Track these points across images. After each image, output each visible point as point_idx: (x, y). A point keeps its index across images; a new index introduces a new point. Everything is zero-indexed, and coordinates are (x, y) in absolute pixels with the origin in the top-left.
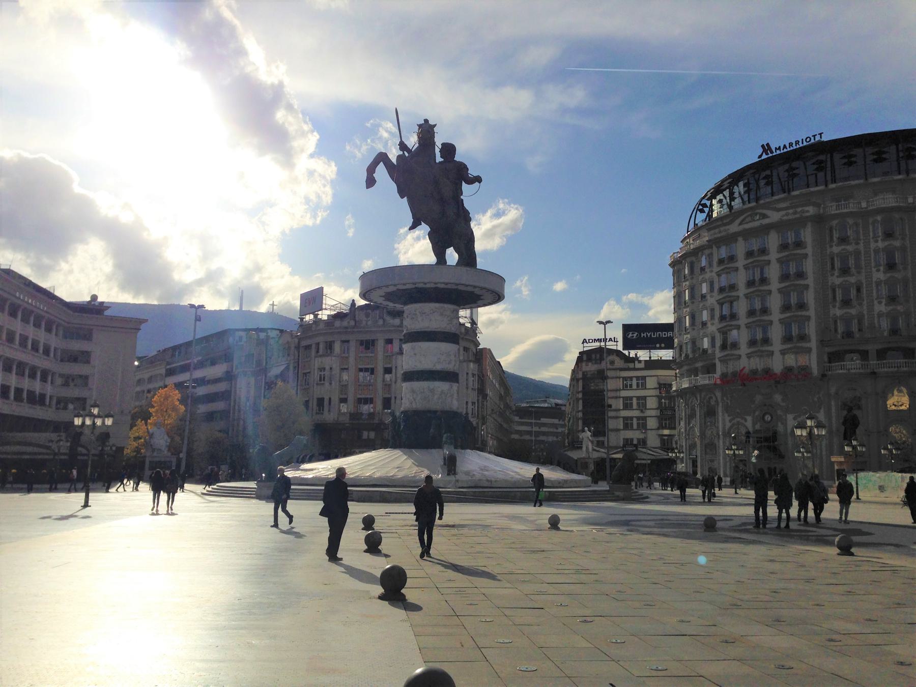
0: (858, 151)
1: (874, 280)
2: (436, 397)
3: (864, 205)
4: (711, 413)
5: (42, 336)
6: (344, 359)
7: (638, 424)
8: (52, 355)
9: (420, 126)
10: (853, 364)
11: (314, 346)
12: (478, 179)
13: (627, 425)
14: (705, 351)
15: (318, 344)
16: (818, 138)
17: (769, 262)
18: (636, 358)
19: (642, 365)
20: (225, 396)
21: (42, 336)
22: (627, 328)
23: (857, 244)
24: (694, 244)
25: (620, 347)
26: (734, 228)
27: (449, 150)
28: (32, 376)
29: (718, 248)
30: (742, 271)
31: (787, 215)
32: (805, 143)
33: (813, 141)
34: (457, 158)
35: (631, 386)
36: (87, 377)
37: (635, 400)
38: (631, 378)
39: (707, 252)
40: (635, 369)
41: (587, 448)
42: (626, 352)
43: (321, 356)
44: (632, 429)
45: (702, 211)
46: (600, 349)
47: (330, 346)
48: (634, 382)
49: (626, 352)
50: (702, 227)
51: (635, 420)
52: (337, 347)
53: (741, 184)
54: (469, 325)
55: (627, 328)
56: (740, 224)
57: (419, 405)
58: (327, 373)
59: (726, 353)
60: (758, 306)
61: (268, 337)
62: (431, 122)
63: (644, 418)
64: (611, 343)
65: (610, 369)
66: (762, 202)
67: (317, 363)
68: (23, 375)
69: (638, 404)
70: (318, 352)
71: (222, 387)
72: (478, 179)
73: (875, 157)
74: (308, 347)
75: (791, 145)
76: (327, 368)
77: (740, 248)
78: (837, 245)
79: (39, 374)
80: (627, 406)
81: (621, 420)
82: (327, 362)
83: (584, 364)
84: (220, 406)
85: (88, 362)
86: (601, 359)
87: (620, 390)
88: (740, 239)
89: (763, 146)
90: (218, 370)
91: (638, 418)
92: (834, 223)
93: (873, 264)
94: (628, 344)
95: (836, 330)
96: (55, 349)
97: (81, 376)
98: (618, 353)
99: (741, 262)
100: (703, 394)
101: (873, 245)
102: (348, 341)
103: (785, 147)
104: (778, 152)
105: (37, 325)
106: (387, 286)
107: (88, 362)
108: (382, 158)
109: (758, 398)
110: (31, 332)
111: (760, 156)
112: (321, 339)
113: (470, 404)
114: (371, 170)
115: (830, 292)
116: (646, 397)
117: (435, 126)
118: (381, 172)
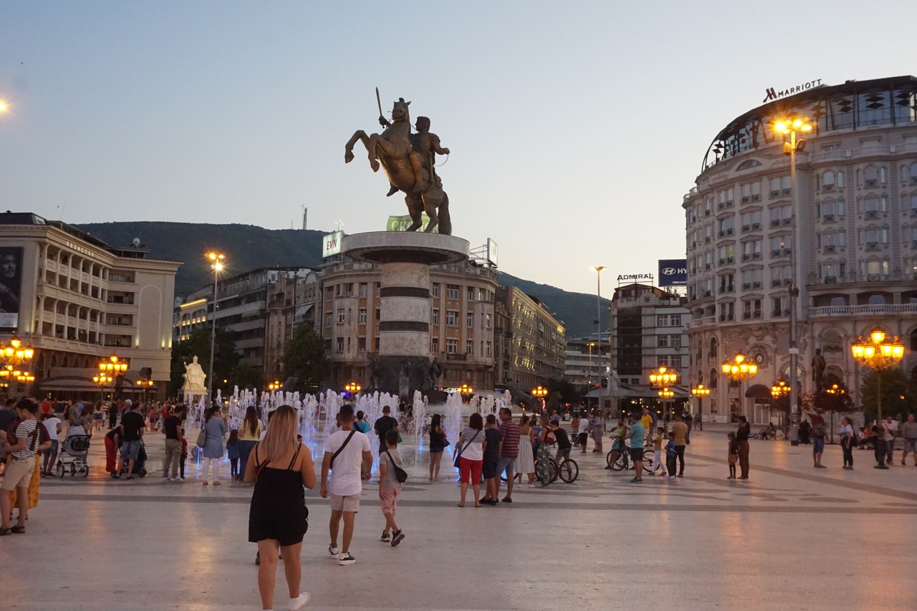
0: (850, 98)
1: (856, 227)
2: (406, 344)
3: (848, 154)
4: (713, 354)
5: (90, 279)
6: (363, 301)
7: (673, 362)
8: (100, 296)
9: (396, 104)
10: (835, 309)
11: (335, 288)
12: (446, 151)
14: (708, 294)
15: (339, 286)
16: (816, 85)
17: (761, 209)
18: (676, 296)
19: (677, 302)
20: (260, 332)
21: (90, 279)
22: (663, 264)
23: (841, 191)
24: (705, 186)
25: (656, 283)
26: (732, 174)
27: (423, 123)
28: (83, 317)
29: (719, 192)
30: (766, 211)
31: (777, 163)
32: (805, 89)
33: (812, 87)
34: (431, 131)
35: (666, 323)
36: (131, 316)
37: (669, 338)
38: (666, 316)
39: (710, 195)
40: (669, 306)
41: (611, 387)
42: (662, 288)
43: (342, 297)
45: (717, 151)
46: (636, 287)
47: (349, 287)
48: (669, 319)
49: (662, 288)
50: (713, 167)
51: (669, 357)
52: (356, 287)
53: (749, 127)
54: (486, 266)
55: (663, 264)
56: (738, 170)
57: (391, 351)
58: (346, 313)
59: (723, 296)
60: (748, 251)
61: (296, 278)
62: (406, 102)
63: (679, 356)
64: (646, 279)
65: (646, 307)
66: (759, 148)
67: (337, 303)
68: (75, 316)
69: (672, 341)
70: (339, 293)
71: (256, 324)
72: (446, 151)
73: (870, 103)
74: (330, 289)
75: (792, 90)
76: (347, 309)
77: (732, 195)
78: (824, 192)
79: (89, 315)
80: (662, 344)
82: (347, 303)
83: (619, 301)
84: (256, 342)
85: (131, 302)
86: (636, 296)
87: (655, 328)
88: (737, 185)
89: (768, 90)
90: (252, 308)
91: (673, 356)
92: (820, 171)
93: (856, 212)
94: (665, 280)
95: (820, 277)
96: (103, 290)
97: (126, 315)
98: (653, 288)
99: (738, 207)
100: (707, 334)
101: (856, 194)
102: (366, 284)
103: (787, 92)
104: (781, 97)
105: (85, 269)
106: (362, 249)
107: (131, 302)
108: (360, 135)
109: (752, 341)
110: (80, 276)
111: (765, 101)
112: (340, 281)
113: (485, 343)
114: (350, 146)
115: (816, 236)
116: (680, 335)
117: (409, 103)
118: (360, 148)
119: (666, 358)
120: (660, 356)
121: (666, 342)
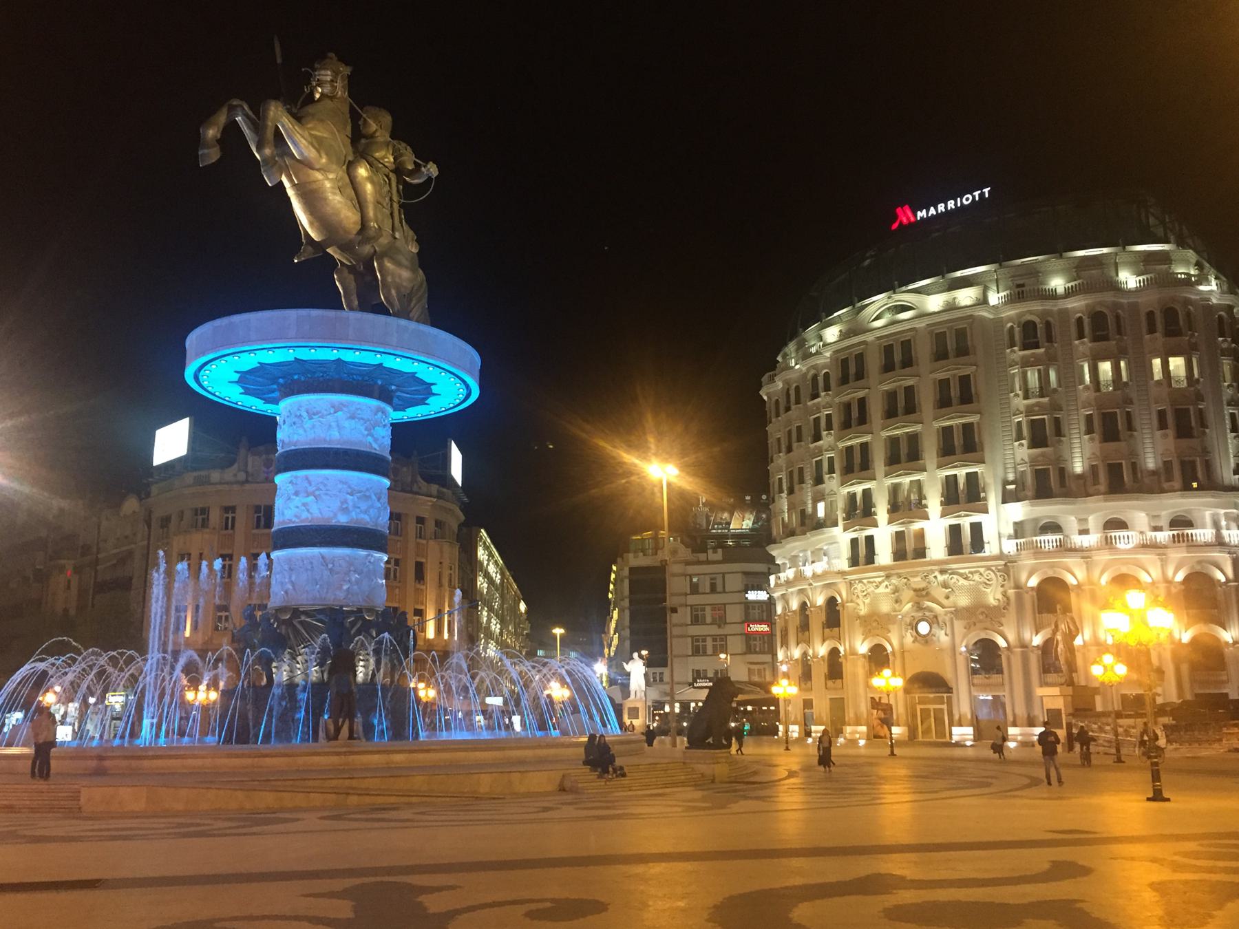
13: (698, 651)
19: (719, 555)
40: (708, 562)
44: (705, 654)
51: (709, 640)
52: (215, 517)
63: (724, 638)
80: (697, 620)
81: (689, 640)
87: (686, 595)
102: (232, 509)
119: (704, 641)
120: (695, 639)
121: (704, 616)
